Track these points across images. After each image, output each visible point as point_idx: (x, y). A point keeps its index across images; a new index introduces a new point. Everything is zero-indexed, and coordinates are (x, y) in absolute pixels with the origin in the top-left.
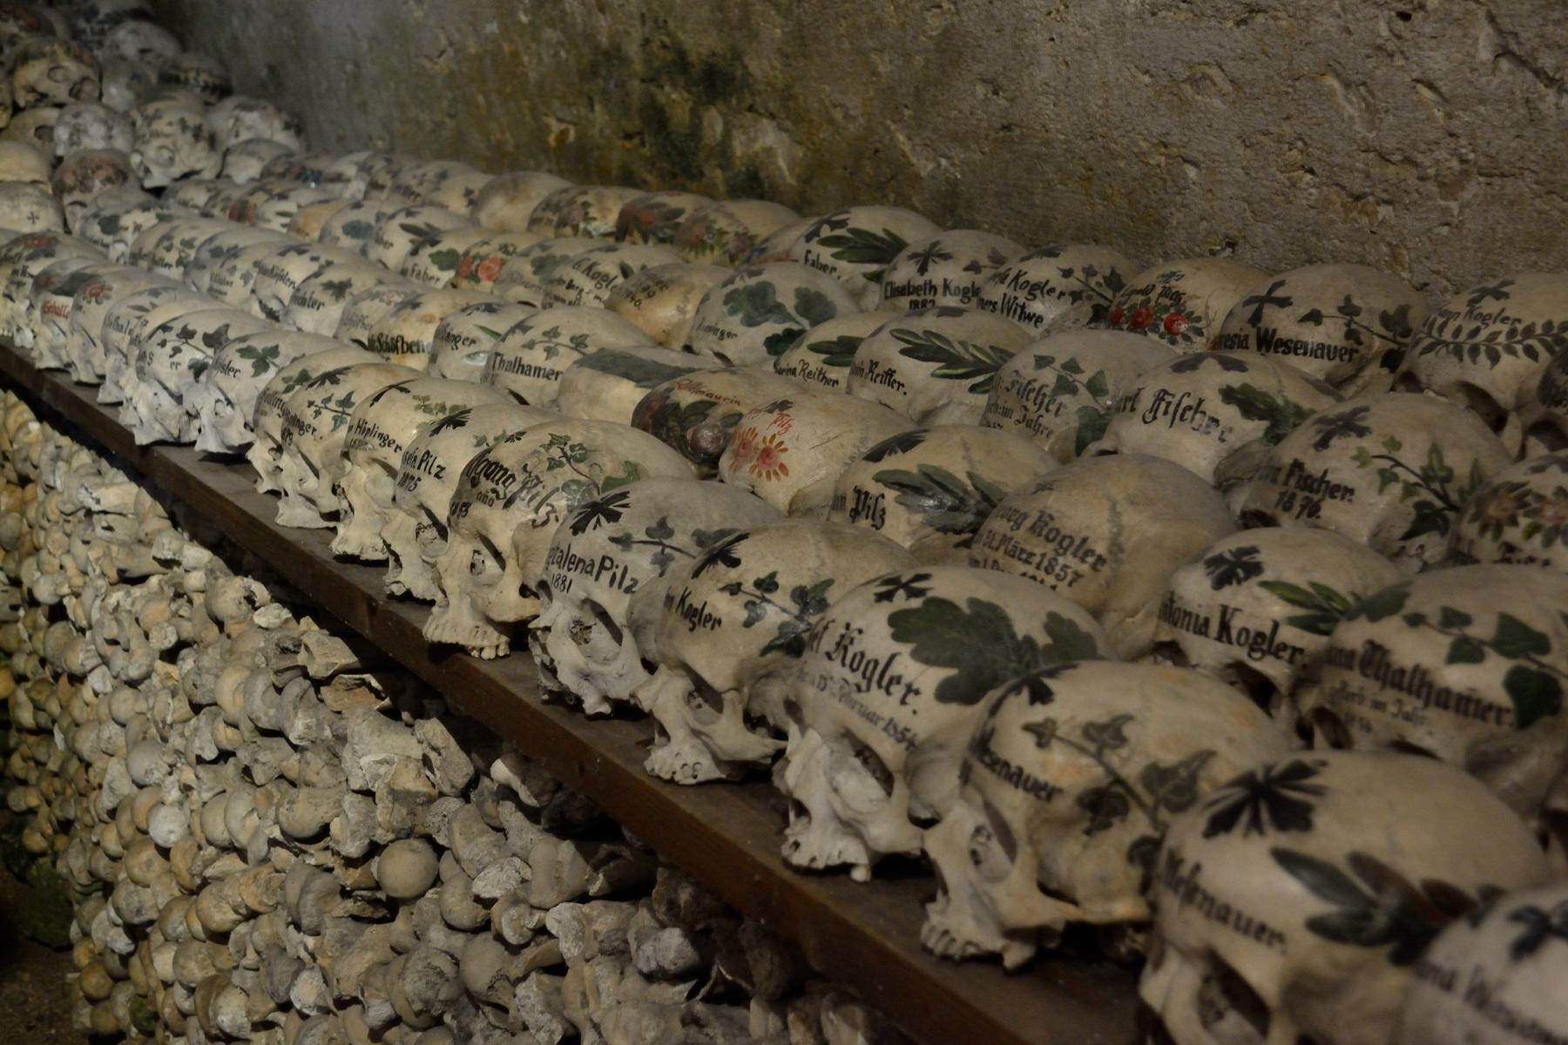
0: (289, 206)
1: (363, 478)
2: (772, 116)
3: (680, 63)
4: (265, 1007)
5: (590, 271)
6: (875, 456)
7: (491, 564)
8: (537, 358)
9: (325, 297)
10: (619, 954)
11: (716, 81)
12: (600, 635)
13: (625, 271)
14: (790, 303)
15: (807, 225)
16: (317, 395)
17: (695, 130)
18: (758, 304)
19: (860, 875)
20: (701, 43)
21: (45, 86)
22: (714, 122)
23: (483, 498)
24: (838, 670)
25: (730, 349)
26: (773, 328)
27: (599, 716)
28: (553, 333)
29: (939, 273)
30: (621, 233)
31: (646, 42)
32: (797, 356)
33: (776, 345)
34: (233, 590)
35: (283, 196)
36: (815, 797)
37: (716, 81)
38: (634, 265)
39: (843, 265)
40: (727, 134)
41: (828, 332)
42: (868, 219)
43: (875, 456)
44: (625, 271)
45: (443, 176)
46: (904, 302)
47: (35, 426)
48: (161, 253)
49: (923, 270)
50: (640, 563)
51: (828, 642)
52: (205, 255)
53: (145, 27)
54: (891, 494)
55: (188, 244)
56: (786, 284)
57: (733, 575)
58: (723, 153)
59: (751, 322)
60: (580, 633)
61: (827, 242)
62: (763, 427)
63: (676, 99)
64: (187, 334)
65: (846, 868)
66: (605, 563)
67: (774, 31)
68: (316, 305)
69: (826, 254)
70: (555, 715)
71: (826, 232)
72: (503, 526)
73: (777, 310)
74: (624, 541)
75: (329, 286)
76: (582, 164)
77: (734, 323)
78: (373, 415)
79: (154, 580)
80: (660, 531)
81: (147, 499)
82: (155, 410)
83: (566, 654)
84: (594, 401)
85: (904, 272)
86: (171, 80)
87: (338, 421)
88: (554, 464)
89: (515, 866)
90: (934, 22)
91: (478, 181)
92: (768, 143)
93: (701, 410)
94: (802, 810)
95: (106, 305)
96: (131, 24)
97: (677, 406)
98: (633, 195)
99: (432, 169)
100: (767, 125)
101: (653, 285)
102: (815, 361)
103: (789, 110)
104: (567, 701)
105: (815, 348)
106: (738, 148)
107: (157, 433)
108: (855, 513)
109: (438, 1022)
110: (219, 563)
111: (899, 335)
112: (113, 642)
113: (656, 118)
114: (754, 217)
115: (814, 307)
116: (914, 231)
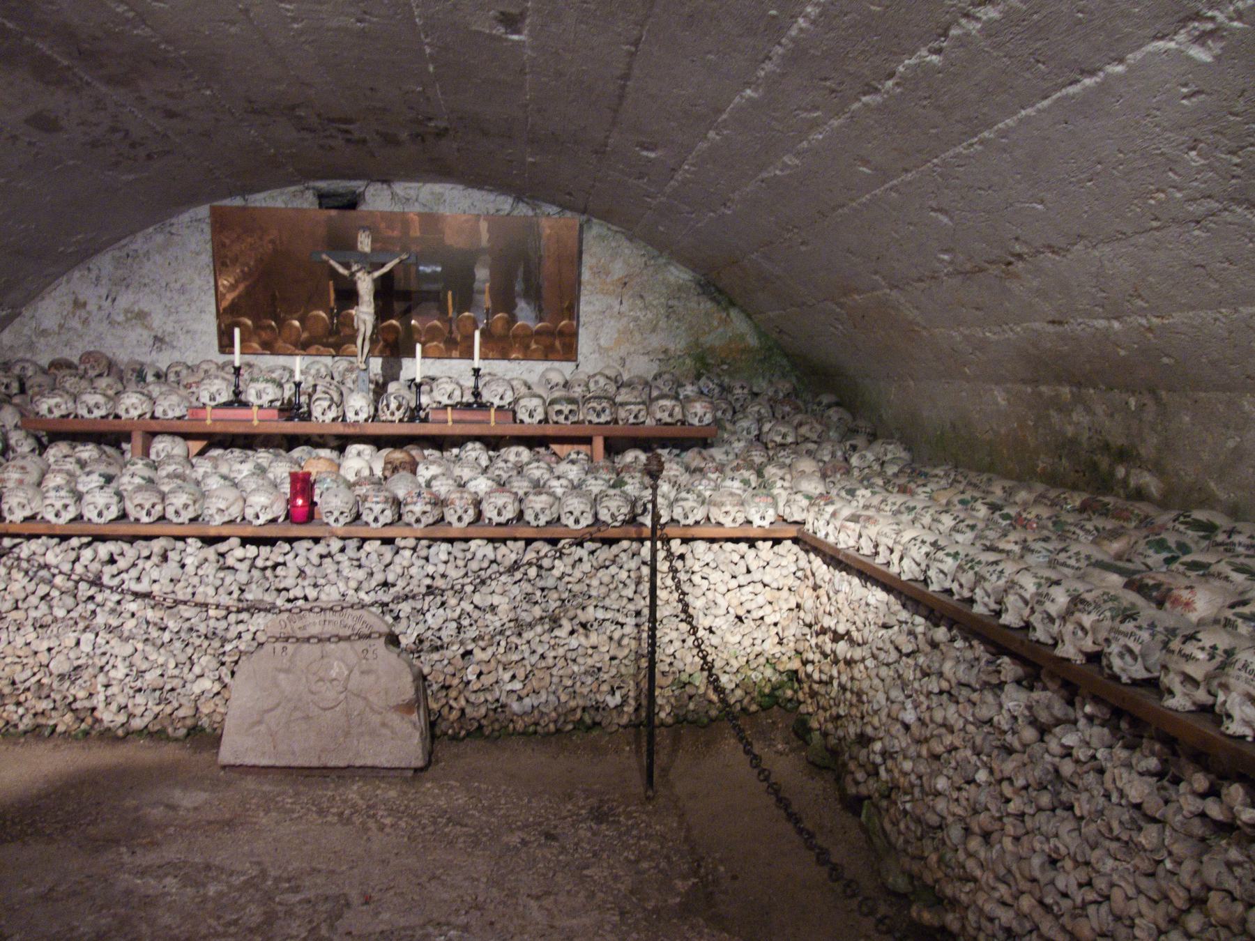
0: (928, 489)
1: (1011, 600)
2: (1149, 471)
3: (1106, 447)
4: (959, 781)
5: (1082, 528)
6: (1232, 606)
7: (1080, 633)
8: (1072, 562)
9: (968, 530)
10: (1128, 765)
11: (1124, 455)
12: (1128, 658)
13: (1097, 529)
14: (1173, 546)
15: (1173, 514)
16: (991, 569)
17: (1112, 474)
18: (1161, 545)
19: (1249, 739)
20: (1118, 440)
21: (808, 435)
22: (1121, 472)
23: (1079, 610)
24: (1243, 674)
25: (1149, 562)
26: (1165, 555)
27: (1126, 684)
28: (1078, 553)
29: (1236, 539)
30: (1083, 509)
31: (1090, 438)
32: (1174, 566)
33: (1168, 561)
34: (941, 633)
35: (924, 485)
36: (1236, 713)
37: (1124, 455)
38: (1100, 526)
39: (1190, 532)
40: (1127, 474)
41: (1188, 558)
42: (1200, 515)
43: (1232, 606)
44: (1097, 529)
45: (990, 480)
46: (1222, 548)
47: (825, 567)
48: (883, 506)
49: (1229, 537)
50: (1145, 635)
51: (1239, 665)
52: (903, 509)
53: (841, 410)
54: (1240, 621)
55: (894, 504)
56: (1171, 540)
57: (1200, 644)
58: (1125, 482)
59: (1157, 552)
60: (1121, 656)
61: (1182, 523)
62: (1185, 595)
63: (1104, 462)
64: (923, 542)
65: (1243, 737)
66: (1132, 634)
67: (1154, 440)
68: (963, 532)
69: (1182, 528)
70: (1112, 683)
71: (1182, 519)
72: (1087, 620)
73: (1169, 549)
74: (1140, 628)
75: (968, 526)
76: (1052, 479)
77: (1151, 552)
78: (1016, 578)
79: (896, 628)
80: (1152, 626)
81: (892, 598)
82: (910, 568)
83: (1117, 663)
84: (1103, 580)
85: (1221, 537)
86: (854, 431)
87: (999, 578)
88: (1105, 601)
89: (1083, 736)
90: (1231, 444)
91: (1008, 484)
92: (1151, 483)
93: (1158, 586)
94: (1229, 716)
95: (878, 527)
96: (835, 409)
97: (1147, 585)
98: (1085, 496)
99: (985, 477)
100: (1146, 473)
101: (1115, 535)
102: (1182, 568)
103: (1158, 468)
104: (1117, 678)
105: (1183, 564)
106: (1132, 483)
107: (910, 576)
108: (1225, 626)
109: (1045, 788)
110: (929, 624)
111: (1230, 564)
112: (880, 649)
113: (1094, 466)
114: (1142, 508)
115: (1184, 548)
116: (1221, 520)
